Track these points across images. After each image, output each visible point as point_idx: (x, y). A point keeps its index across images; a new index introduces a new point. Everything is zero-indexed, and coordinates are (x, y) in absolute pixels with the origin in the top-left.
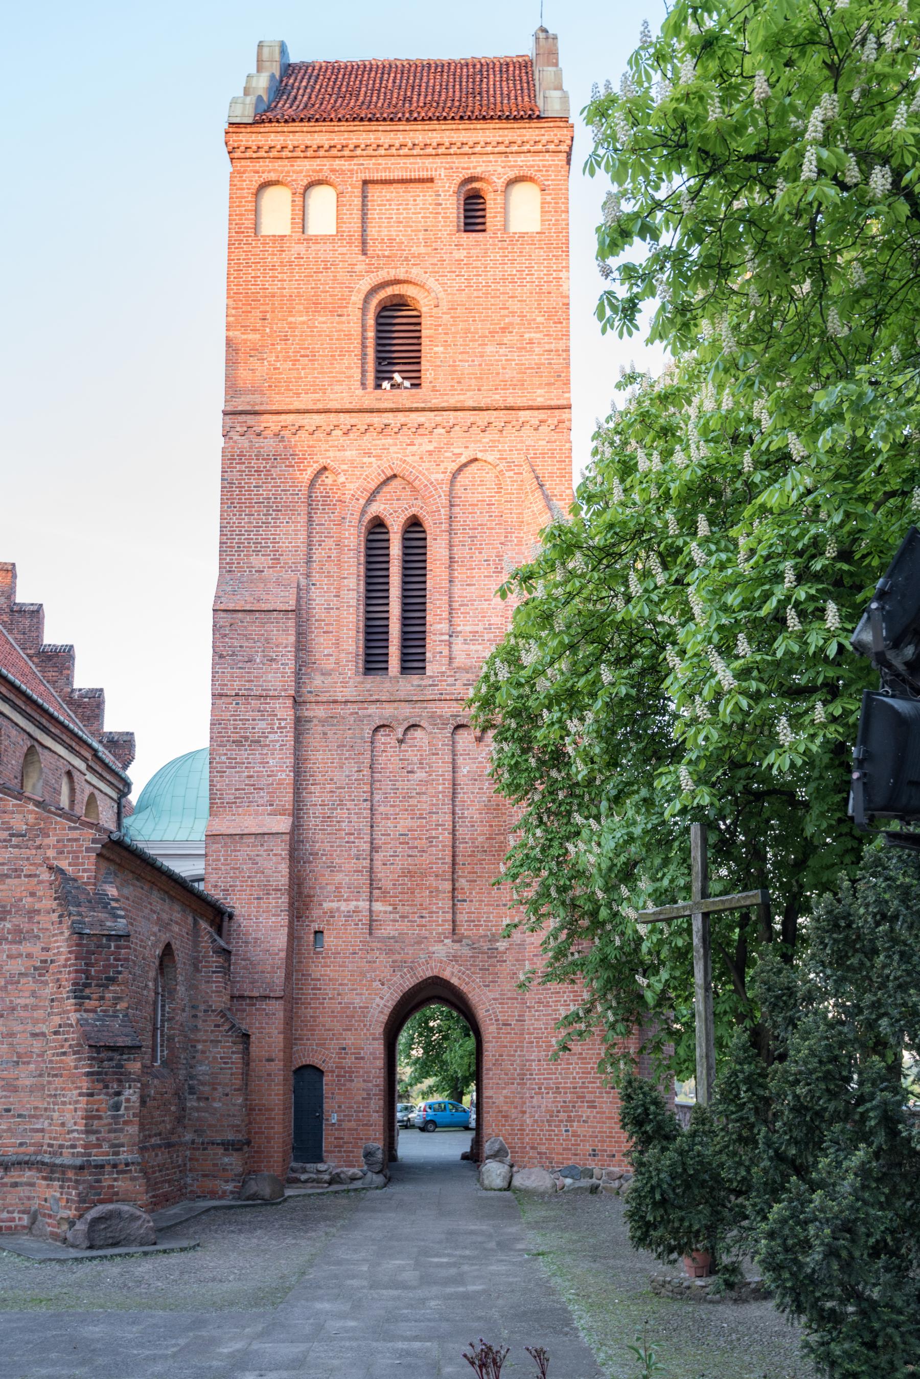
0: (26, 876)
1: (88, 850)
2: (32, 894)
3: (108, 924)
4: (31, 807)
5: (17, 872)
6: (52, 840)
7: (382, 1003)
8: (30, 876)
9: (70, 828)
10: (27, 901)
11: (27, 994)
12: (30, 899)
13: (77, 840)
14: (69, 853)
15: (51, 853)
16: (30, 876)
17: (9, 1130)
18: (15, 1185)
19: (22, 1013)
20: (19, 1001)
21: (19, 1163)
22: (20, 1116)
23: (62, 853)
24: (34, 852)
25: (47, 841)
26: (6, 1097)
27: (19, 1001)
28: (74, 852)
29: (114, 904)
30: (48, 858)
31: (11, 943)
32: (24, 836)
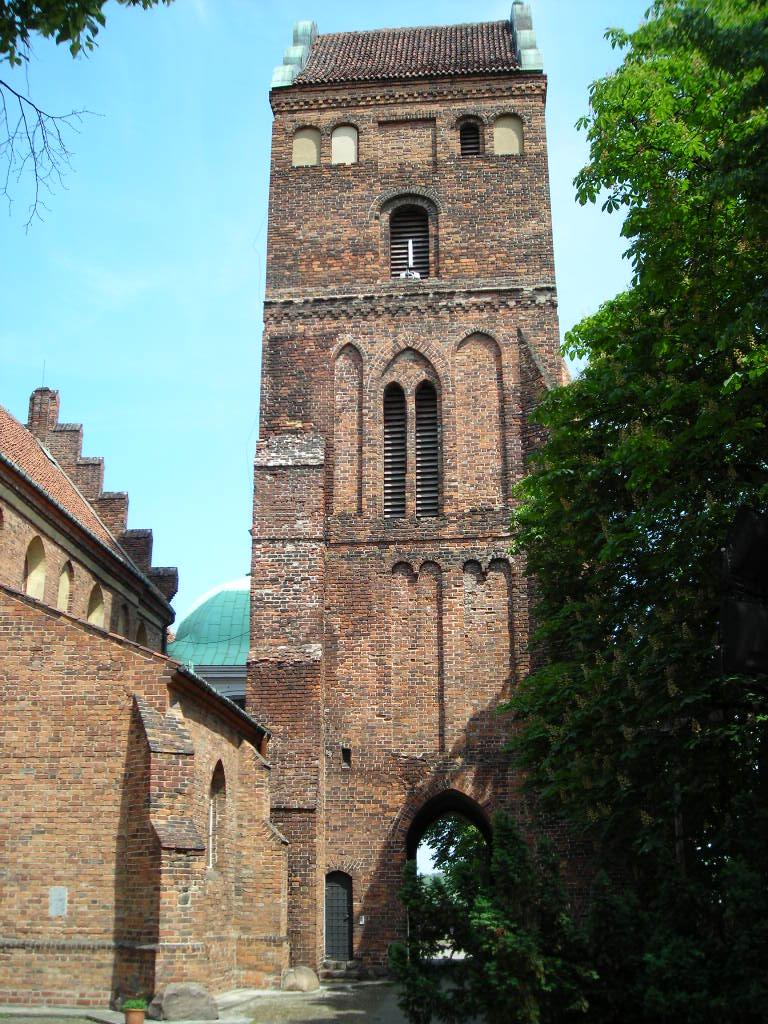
0: (111, 703)
1: (161, 681)
3: (177, 744)
4: (115, 644)
5: (103, 700)
6: (131, 673)
8: (113, 703)
9: (147, 663)
11: (110, 803)
12: (112, 722)
13: (151, 672)
14: (144, 683)
15: (130, 683)
16: (113, 703)
17: (95, 919)
19: (107, 820)
20: (103, 808)
21: (104, 947)
22: (104, 907)
23: (139, 683)
24: (117, 682)
25: (127, 673)
26: (93, 891)
27: (103, 808)
28: (149, 682)
29: (180, 726)
30: (128, 688)
31: (99, 758)
32: (108, 669)
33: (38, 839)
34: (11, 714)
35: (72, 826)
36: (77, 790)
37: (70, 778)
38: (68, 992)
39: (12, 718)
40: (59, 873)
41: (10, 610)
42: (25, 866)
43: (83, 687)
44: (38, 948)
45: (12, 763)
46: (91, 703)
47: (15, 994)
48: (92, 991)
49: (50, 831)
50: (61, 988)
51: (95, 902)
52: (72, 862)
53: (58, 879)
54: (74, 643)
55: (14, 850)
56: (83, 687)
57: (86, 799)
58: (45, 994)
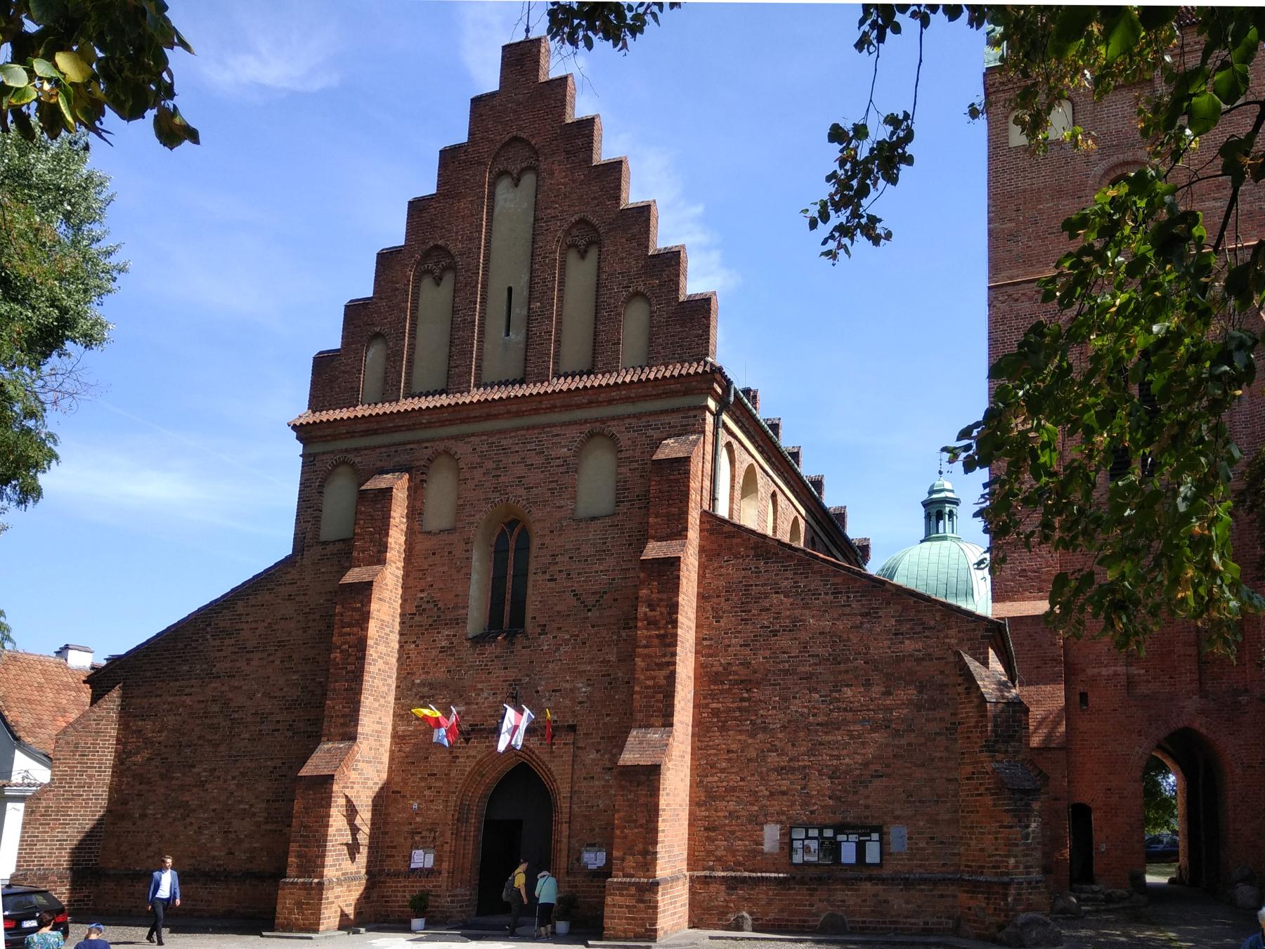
2: (942, 672)
7: (1141, 751)
10: (938, 678)
18: (942, 896)
22: (942, 843)
31: (929, 709)
33: (877, 783)
34: (847, 672)
35: (907, 771)
36: (911, 738)
37: (903, 727)
38: (913, 921)
39: (845, 677)
40: (897, 813)
41: (838, 580)
42: (867, 807)
43: (909, 646)
44: (883, 881)
45: (849, 716)
46: (919, 660)
47: (864, 922)
48: (935, 920)
49: (889, 776)
50: (907, 917)
51: (932, 838)
52: (910, 802)
53: (897, 818)
54: (899, 608)
55: (855, 793)
56: (909, 646)
57: (920, 745)
58: (891, 922)
